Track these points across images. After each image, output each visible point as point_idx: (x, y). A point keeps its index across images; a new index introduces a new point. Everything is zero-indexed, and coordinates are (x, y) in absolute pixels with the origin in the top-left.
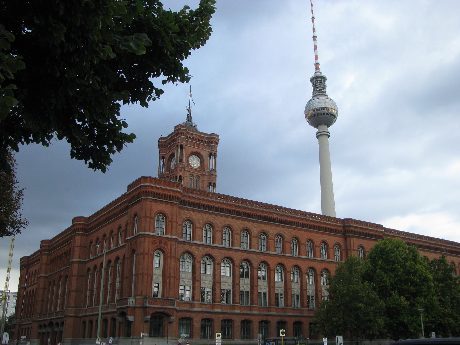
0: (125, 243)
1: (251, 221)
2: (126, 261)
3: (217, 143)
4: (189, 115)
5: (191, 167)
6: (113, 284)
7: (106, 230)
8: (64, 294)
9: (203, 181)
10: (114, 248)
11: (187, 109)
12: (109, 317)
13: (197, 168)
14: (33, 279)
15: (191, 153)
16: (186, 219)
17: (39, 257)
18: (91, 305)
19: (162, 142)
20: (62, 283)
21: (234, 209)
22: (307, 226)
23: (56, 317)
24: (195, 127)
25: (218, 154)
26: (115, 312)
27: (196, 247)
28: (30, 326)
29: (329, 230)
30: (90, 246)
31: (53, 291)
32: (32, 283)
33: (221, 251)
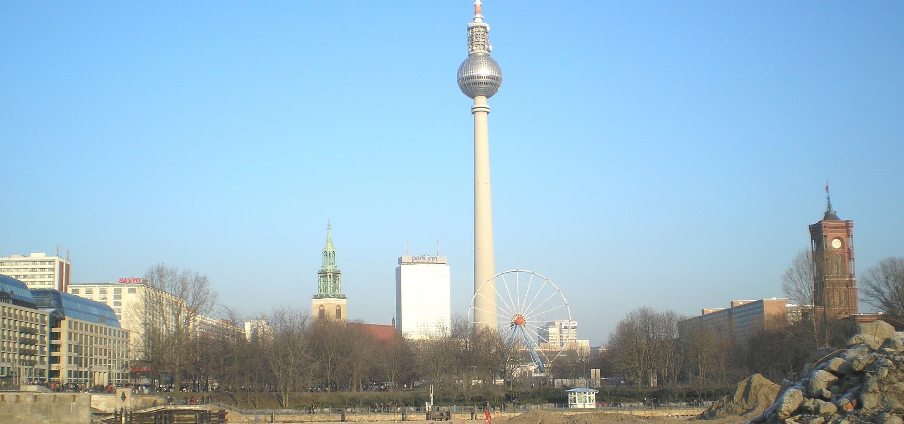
3: (852, 227)
13: (839, 248)
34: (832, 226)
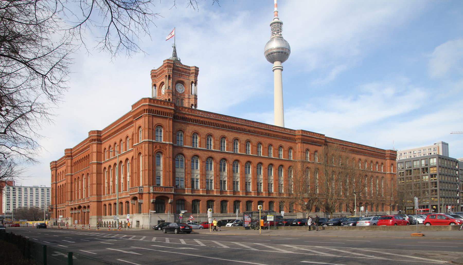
0: (133, 148)
1: (228, 131)
2: (134, 161)
4: (175, 51)
6: (125, 178)
7: (116, 139)
8: (87, 186)
10: (124, 152)
11: (173, 47)
12: (124, 201)
14: (62, 177)
15: (177, 82)
16: (178, 129)
17: (64, 161)
18: (109, 193)
19: (153, 73)
20: (85, 179)
21: (215, 122)
22: (269, 135)
23: (83, 203)
24: (179, 61)
25: (198, 82)
26: (129, 197)
27: (187, 150)
28: (64, 209)
29: (285, 138)
30: (104, 152)
31: (78, 184)
32: (62, 180)
33: (206, 153)
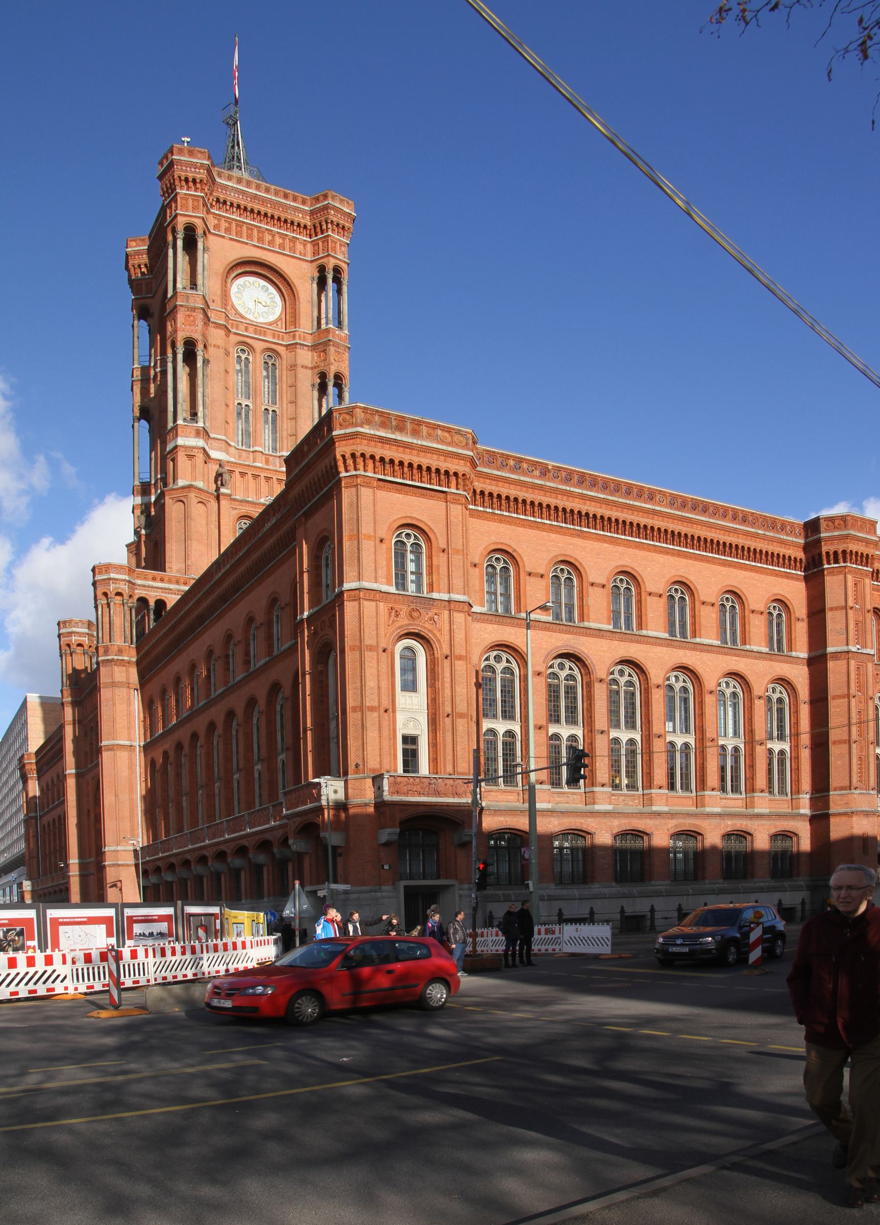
5: (243, 317)
9: (293, 367)
13: (271, 324)
34: (232, 197)
